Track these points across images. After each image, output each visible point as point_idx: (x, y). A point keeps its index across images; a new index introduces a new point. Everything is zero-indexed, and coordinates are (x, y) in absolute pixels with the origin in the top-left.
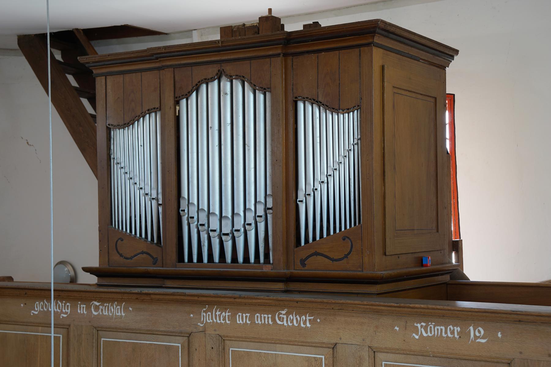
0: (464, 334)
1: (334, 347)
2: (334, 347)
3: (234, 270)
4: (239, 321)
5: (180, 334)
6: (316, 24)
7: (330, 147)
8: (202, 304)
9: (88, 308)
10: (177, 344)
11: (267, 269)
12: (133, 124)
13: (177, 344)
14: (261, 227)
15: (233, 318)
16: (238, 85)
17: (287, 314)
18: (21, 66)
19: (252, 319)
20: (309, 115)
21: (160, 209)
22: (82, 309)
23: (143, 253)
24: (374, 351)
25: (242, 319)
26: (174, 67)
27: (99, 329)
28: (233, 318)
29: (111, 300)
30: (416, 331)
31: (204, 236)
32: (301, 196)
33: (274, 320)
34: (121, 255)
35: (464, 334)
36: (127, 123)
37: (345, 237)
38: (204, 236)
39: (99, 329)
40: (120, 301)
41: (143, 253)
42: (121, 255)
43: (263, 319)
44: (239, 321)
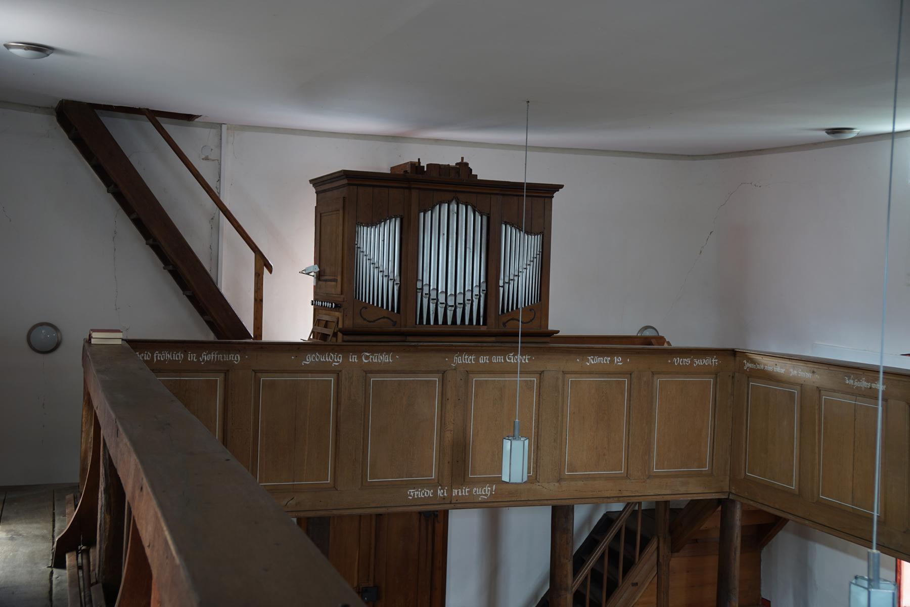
0: (612, 361)
1: (541, 373)
2: (541, 373)
3: (428, 329)
4: (481, 361)
5: (437, 372)
6: (463, 167)
8: (455, 351)
9: (359, 358)
10: (436, 378)
11: (484, 329)
12: (380, 223)
13: (436, 378)
15: (477, 360)
16: (463, 208)
17: (514, 356)
18: (48, 125)
19: (490, 359)
21: (396, 288)
22: (353, 359)
23: (384, 317)
24: (564, 373)
25: (483, 359)
26: (419, 189)
27: (369, 371)
28: (477, 360)
29: (381, 352)
31: (432, 307)
32: (501, 283)
33: (505, 359)
34: (365, 319)
35: (612, 361)
36: (373, 222)
38: (432, 307)
39: (366, 372)
40: (388, 352)
41: (384, 317)
42: (365, 319)
43: (498, 359)
44: (481, 361)
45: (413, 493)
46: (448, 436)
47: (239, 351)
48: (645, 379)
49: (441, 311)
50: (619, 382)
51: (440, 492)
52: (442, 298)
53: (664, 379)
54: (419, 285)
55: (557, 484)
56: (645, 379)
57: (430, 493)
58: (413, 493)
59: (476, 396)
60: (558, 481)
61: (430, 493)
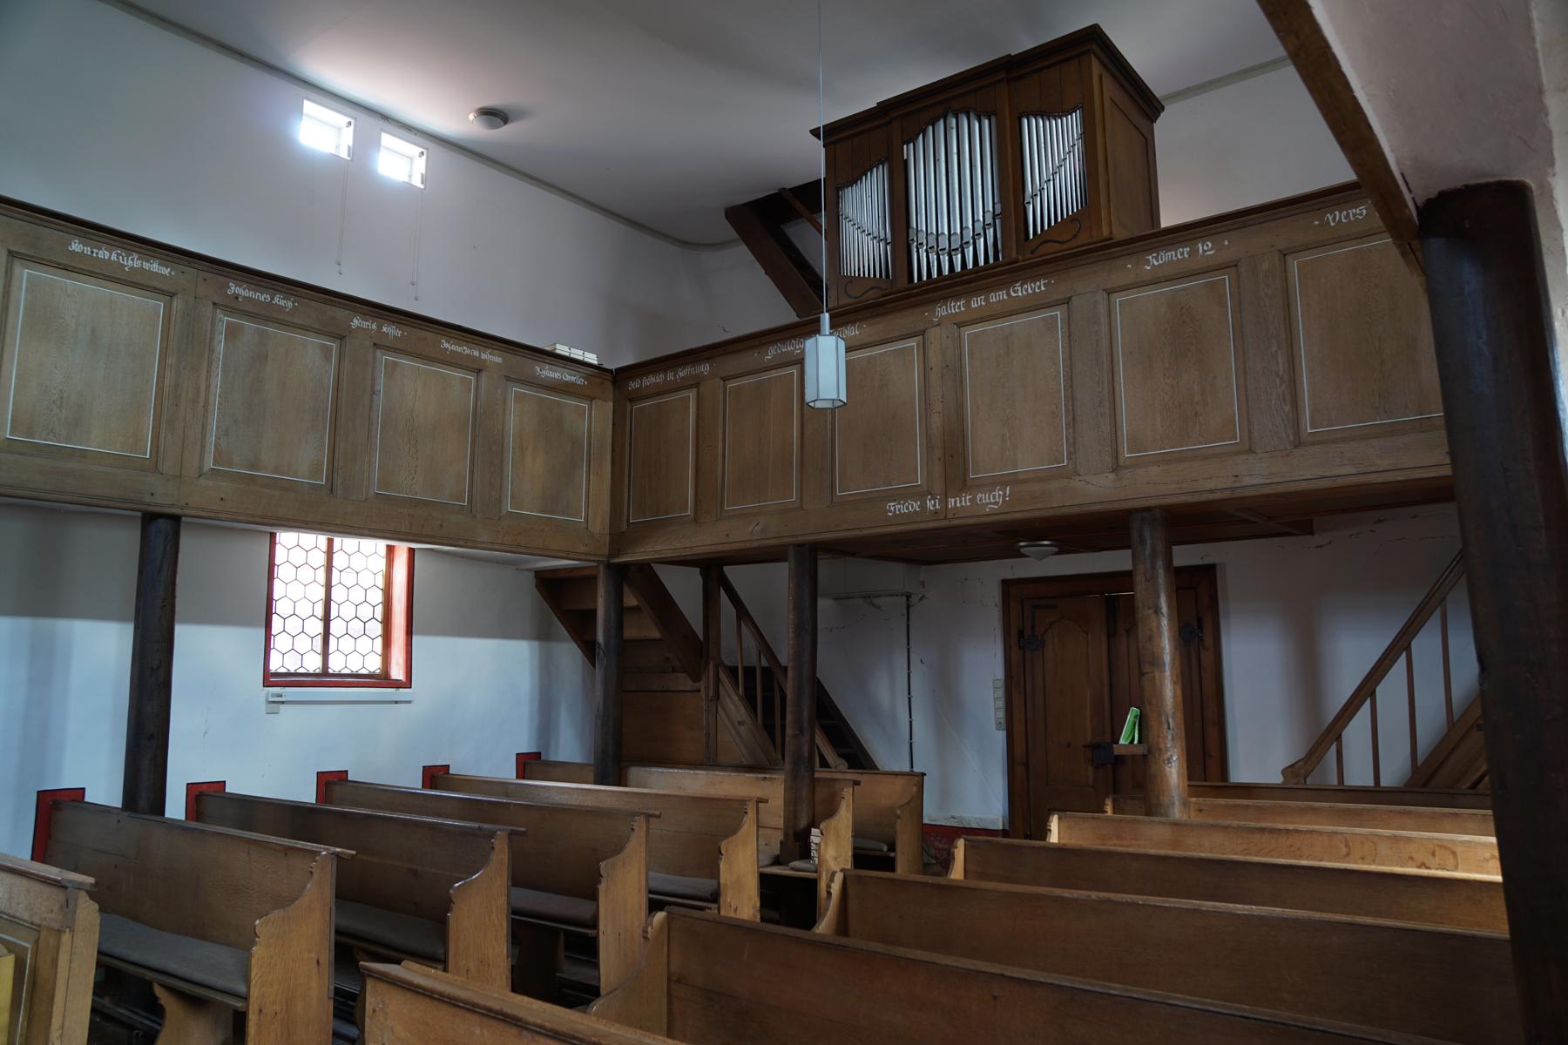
0: (1194, 252)
7: (1054, 153)
8: (935, 301)
14: (990, 232)
15: (968, 305)
20: (1032, 128)
28: (968, 305)
30: (1148, 262)
33: (1008, 294)
37: (1073, 219)
38: (933, 257)
40: (853, 322)
45: (894, 507)
46: (936, 420)
47: (708, 359)
48: (1265, 266)
49: (945, 259)
50: (1212, 285)
51: (930, 504)
52: (944, 243)
53: (1308, 257)
54: (912, 235)
55: (1112, 476)
56: (1265, 266)
57: (916, 506)
58: (894, 507)
59: (971, 357)
60: (1114, 470)
61: (916, 506)
